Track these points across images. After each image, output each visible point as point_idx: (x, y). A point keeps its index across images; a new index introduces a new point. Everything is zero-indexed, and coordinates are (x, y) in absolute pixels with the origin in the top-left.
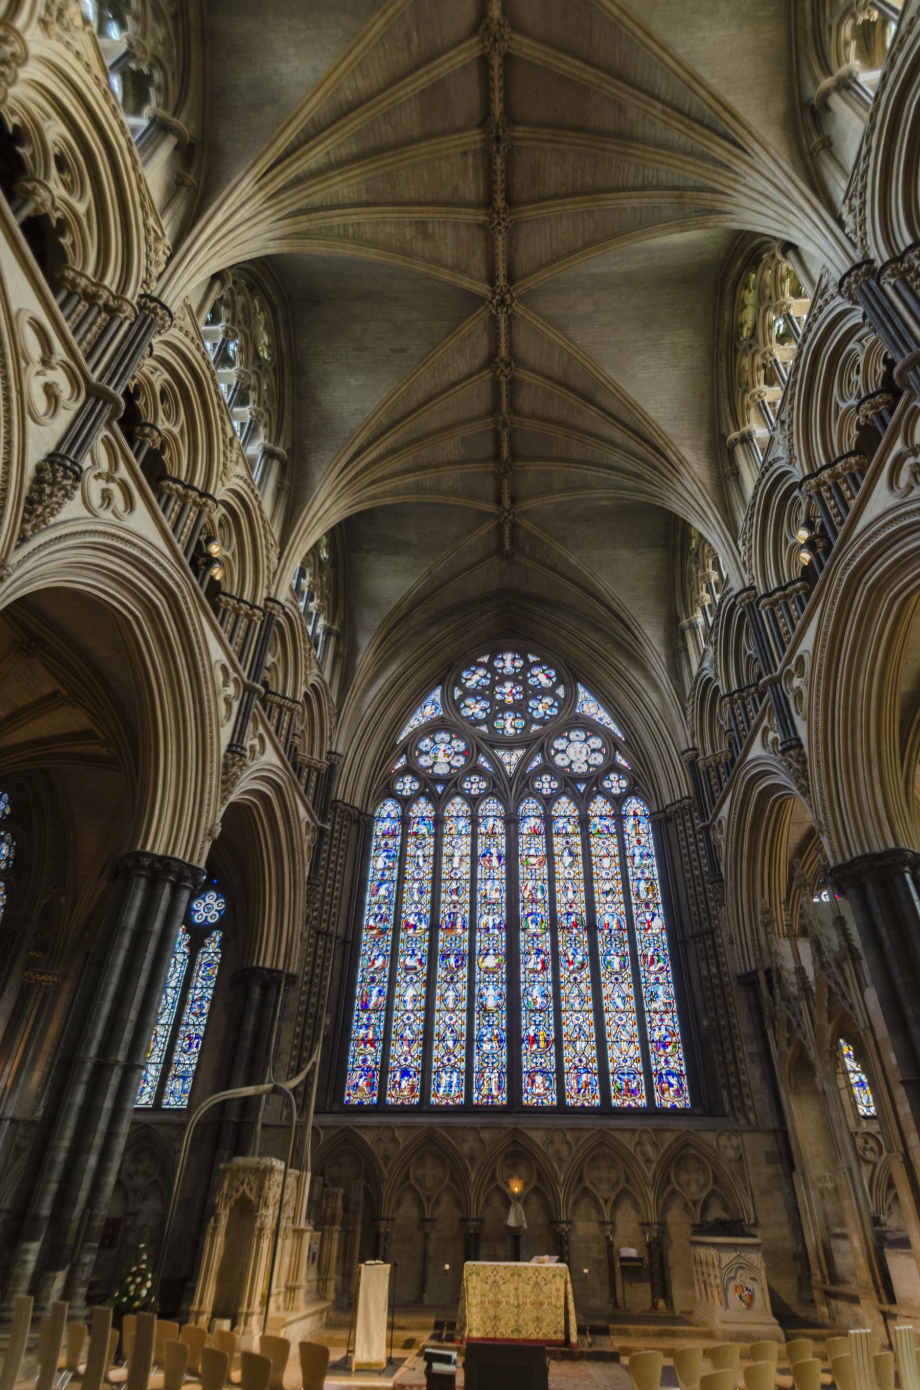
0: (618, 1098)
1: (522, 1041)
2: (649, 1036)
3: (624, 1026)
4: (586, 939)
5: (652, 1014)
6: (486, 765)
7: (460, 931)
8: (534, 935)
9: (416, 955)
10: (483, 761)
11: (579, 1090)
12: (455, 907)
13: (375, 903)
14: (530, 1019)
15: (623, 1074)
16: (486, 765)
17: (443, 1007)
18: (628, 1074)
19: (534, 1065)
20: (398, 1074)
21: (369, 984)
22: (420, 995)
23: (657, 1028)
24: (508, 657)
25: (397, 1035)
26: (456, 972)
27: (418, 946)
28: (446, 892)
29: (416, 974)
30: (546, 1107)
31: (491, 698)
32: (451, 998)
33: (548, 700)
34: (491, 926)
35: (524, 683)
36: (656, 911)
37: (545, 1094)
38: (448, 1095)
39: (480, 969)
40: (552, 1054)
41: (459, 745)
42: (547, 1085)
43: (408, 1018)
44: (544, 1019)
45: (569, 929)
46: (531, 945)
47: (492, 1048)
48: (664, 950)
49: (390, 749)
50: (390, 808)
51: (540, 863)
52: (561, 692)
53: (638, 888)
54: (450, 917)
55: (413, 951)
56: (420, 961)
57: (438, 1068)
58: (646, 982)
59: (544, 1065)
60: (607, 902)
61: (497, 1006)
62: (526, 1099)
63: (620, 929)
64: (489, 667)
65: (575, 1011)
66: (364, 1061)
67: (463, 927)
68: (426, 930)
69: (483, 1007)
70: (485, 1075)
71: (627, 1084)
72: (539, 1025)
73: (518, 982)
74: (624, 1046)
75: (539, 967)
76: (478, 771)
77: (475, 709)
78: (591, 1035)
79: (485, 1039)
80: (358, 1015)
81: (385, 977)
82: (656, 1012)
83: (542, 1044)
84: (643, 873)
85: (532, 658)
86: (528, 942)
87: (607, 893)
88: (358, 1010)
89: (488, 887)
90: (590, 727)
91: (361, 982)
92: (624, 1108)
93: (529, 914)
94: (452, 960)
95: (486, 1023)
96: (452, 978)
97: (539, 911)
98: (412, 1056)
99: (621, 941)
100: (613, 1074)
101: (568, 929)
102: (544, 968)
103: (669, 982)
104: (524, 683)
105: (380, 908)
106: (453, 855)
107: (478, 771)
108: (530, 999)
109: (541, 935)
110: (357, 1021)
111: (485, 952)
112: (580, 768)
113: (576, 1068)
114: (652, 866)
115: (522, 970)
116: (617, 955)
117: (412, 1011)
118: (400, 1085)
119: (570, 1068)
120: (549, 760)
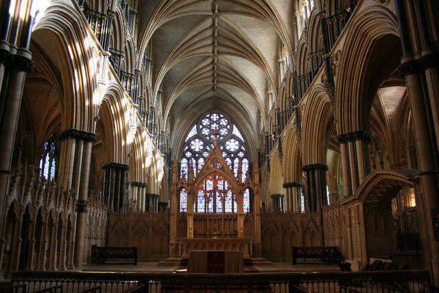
6: (209, 149)
10: (208, 148)
16: (209, 149)
24: (215, 115)
31: (210, 128)
33: (226, 130)
35: (219, 124)
41: (202, 143)
49: (184, 144)
50: (184, 161)
52: (229, 127)
64: (209, 118)
76: (207, 151)
77: (206, 132)
85: (222, 116)
90: (236, 138)
104: (219, 124)
107: (207, 151)
112: (232, 150)
120: (225, 147)
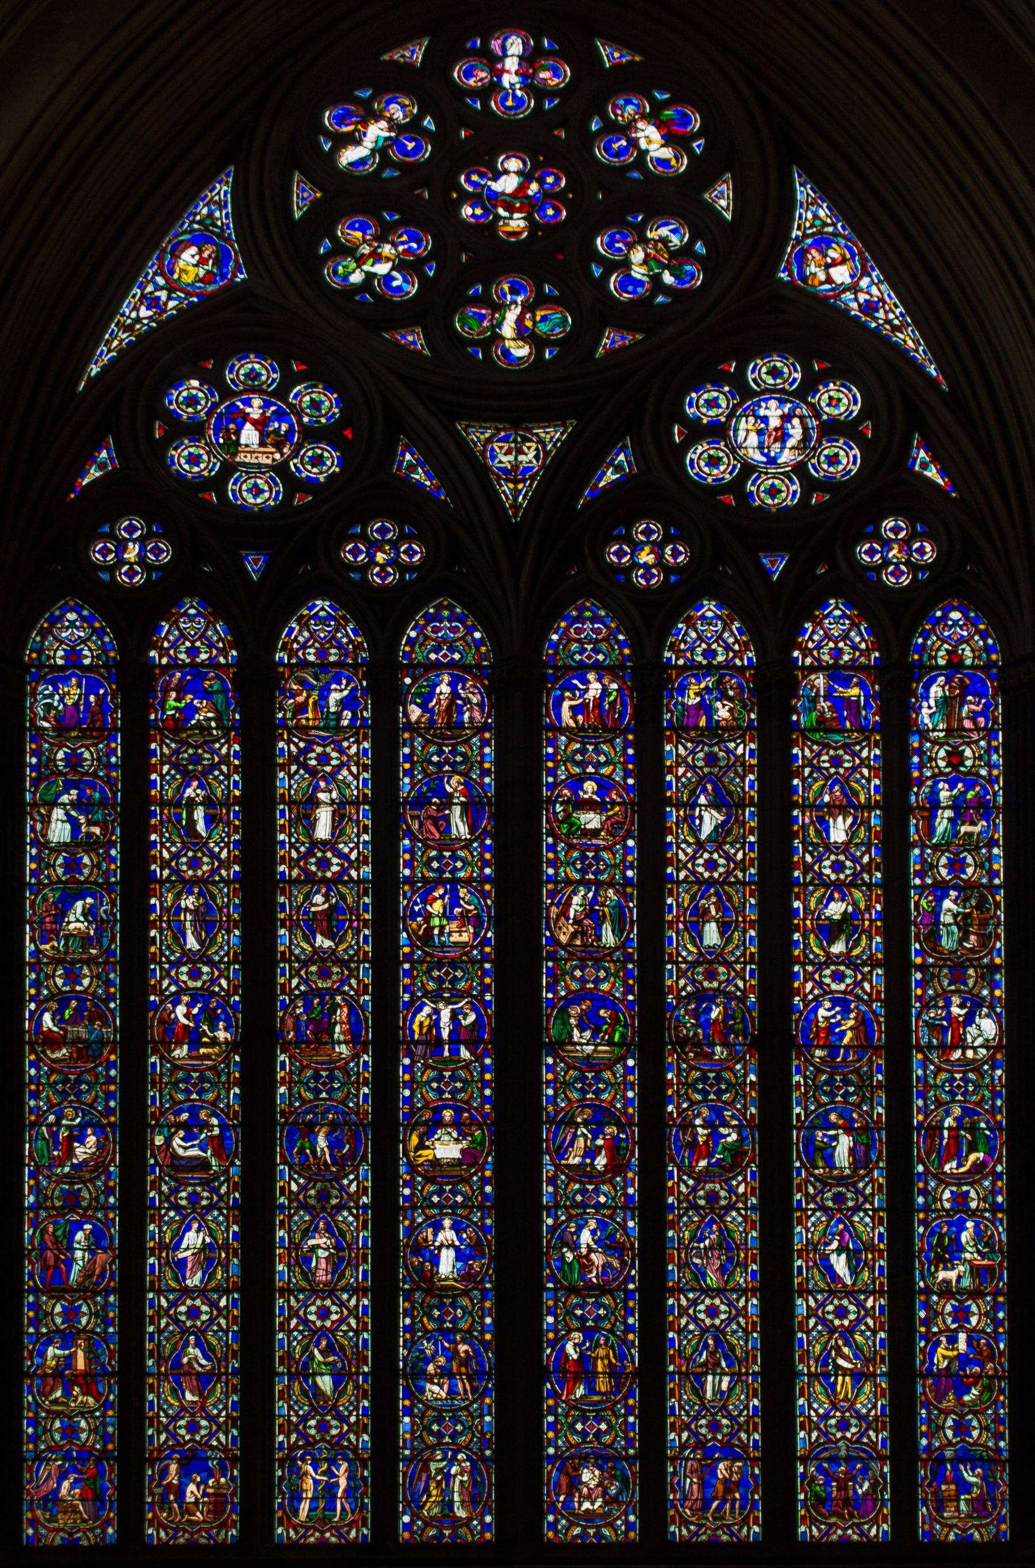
0: (813, 1521)
1: (544, 1374)
2: (919, 1358)
3: (851, 1330)
4: (753, 1077)
5: (935, 1298)
7: (344, 1050)
8: (589, 1063)
9: (206, 1126)
11: (706, 1506)
12: (324, 974)
13: (57, 961)
14: (570, 1313)
15: (834, 1460)
17: (297, 1279)
18: (849, 1460)
19: (575, 1439)
20: (173, 1468)
21: (61, 1212)
22: (226, 1246)
23: (943, 1339)
25: (160, 1361)
26: (338, 1179)
27: (210, 1096)
28: (292, 925)
29: (205, 1183)
30: (610, 1545)
32: (322, 1254)
34: (445, 1034)
36: (985, 992)
37: (608, 1514)
38: (325, 1520)
39: (412, 1168)
40: (630, 1411)
42: (613, 1491)
43: (193, 1313)
44: (611, 1311)
45: (701, 1048)
46: (575, 1096)
47: (452, 1392)
48: (993, 1111)
51: (612, 827)
53: (936, 913)
54: (308, 1007)
55: (193, 1111)
56: (219, 1145)
57: (293, 1448)
58: (926, 1208)
59: (607, 1439)
60: (830, 960)
61: (466, 1276)
62: (552, 1526)
63: (864, 1041)
65: (708, 1291)
66: (70, 1432)
67: (354, 1037)
68: (232, 1046)
69: (427, 1280)
70: (433, 1466)
71: (842, 1487)
72: (597, 1329)
73: (536, 1209)
74: (844, 1384)
75: (601, 1161)
78: (748, 1358)
79: (431, 1368)
80: (35, 1306)
81: (109, 1191)
82: (946, 1291)
83: (602, 1384)
84: (956, 866)
86: (568, 1085)
87: (829, 931)
88: (34, 1290)
89: (437, 907)
91: (35, 1207)
92: (832, 1544)
93: (574, 998)
94: (322, 1142)
95: (431, 1326)
96: (323, 1196)
97: (605, 987)
98: (211, 1418)
99: (865, 1085)
100: (804, 1460)
101: (699, 1044)
102: (616, 1167)
103: (995, 1208)
105: (71, 977)
106: (314, 803)
108: (569, 1256)
109: (610, 1067)
110: (35, 1322)
111: (428, 1115)
113: (700, 1444)
114: (992, 843)
115: (548, 1169)
116: (848, 1130)
117: (201, 1292)
118: (180, 1492)
119: (683, 1447)
